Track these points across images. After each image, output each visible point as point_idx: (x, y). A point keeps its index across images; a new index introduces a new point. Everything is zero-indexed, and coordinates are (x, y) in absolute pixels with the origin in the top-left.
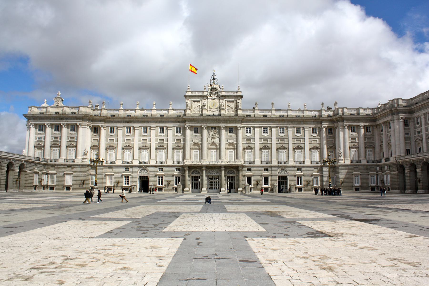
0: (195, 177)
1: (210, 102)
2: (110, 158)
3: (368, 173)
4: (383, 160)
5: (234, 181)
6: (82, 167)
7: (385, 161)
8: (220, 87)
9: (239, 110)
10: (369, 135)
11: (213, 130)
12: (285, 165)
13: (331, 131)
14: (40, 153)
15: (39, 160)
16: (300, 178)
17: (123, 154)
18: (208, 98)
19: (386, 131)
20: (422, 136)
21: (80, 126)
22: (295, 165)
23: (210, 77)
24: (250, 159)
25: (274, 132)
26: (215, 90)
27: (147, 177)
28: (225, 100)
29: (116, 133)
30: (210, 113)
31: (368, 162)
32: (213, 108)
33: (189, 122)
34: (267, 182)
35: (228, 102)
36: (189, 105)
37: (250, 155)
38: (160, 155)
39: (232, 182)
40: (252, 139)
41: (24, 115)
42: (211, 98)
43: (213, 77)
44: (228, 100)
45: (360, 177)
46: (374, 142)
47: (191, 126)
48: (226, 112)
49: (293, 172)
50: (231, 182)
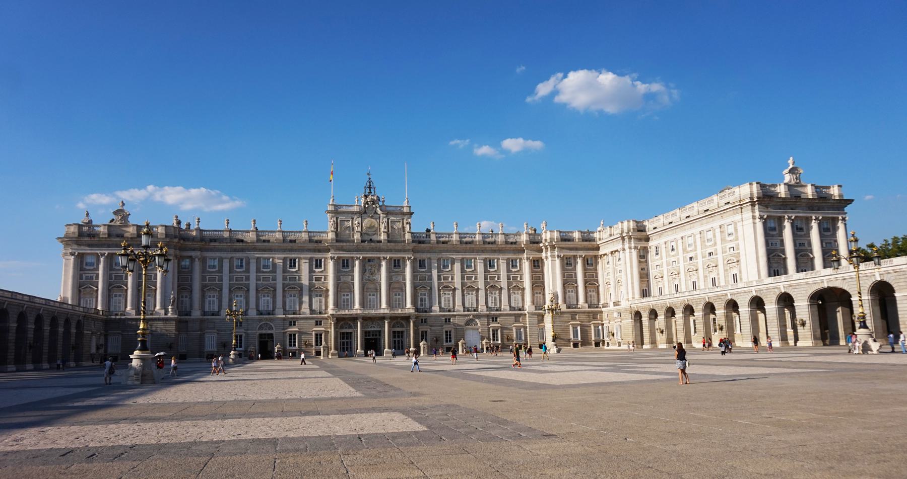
0: (343, 333)
2: (210, 306)
3: (590, 322)
4: (611, 305)
5: (402, 337)
6: (167, 322)
7: (614, 306)
12: (475, 313)
13: (538, 263)
14: (90, 300)
15: (98, 314)
16: (495, 332)
17: (230, 301)
19: (613, 264)
20: (663, 272)
22: (488, 313)
23: (365, 183)
24: (425, 304)
27: (272, 334)
28: (388, 219)
30: (367, 238)
31: (589, 307)
34: (450, 338)
37: (425, 299)
38: (291, 301)
39: (399, 339)
40: (427, 276)
41: (59, 238)
43: (368, 184)
45: (579, 328)
49: (487, 323)
50: (397, 339)
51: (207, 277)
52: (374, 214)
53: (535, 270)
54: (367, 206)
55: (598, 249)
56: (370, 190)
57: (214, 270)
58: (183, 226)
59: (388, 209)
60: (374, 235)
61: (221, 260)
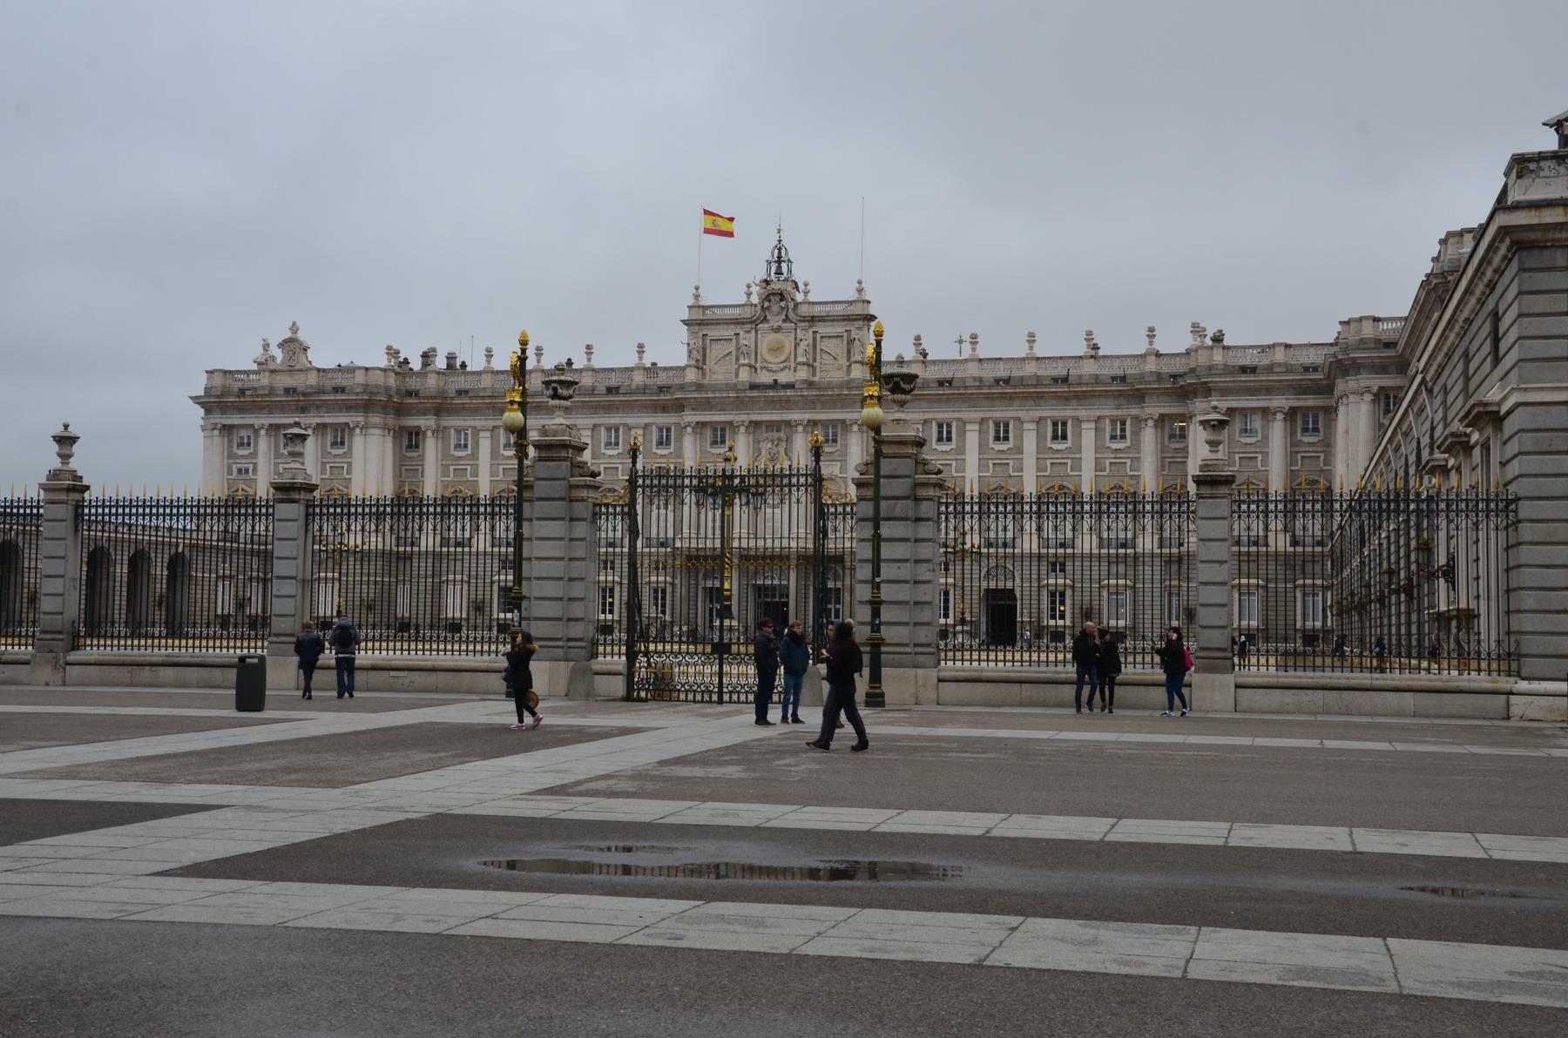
1: (767, 339)
8: (797, 287)
9: (853, 366)
10: (1309, 443)
11: (775, 435)
16: (1057, 596)
18: (760, 326)
21: (358, 431)
23: (767, 253)
25: (972, 438)
26: (781, 300)
29: (472, 448)
30: (765, 378)
31: (1295, 543)
32: (776, 360)
33: (693, 410)
35: (822, 337)
36: (695, 352)
41: (191, 398)
42: (766, 325)
43: (776, 252)
44: (823, 329)
46: (1331, 470)
47: (701, 425)
48: (814, 375)
51: (451, 468)
52: (784, 321)
53: (1173, 446)
54: (766, 304)
55: (1327, 389)
56: (779, 267)
57: (463, 454)
58: (441, 363)
59: (818, 310)
60: (782, 370)
61: (476, 431)
